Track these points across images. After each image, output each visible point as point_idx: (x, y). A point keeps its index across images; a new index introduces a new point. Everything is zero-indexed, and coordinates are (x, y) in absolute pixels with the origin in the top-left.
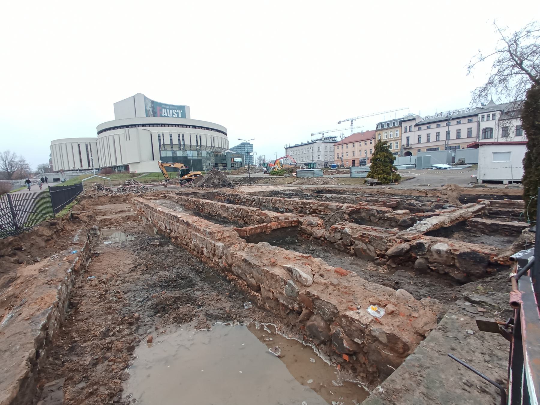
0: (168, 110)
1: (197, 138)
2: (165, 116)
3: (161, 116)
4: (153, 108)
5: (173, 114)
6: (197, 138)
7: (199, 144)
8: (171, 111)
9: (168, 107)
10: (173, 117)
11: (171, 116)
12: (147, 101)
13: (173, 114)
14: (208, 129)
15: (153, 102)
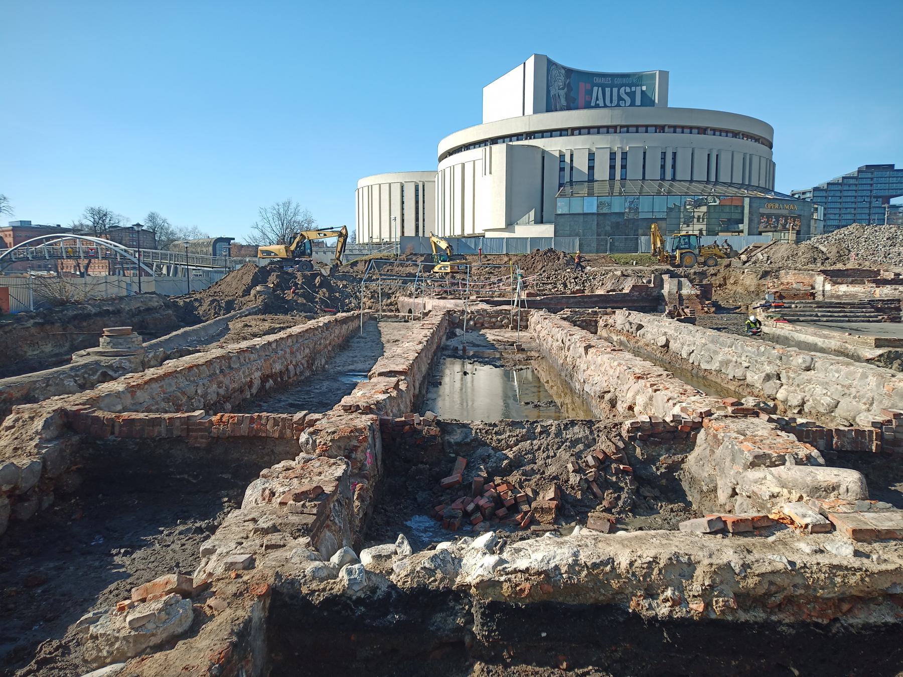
0: (608, 90)
1: (664, 158)
2: (597, 106)
3: (588, 106)
4: (569, 87)
5: (620, 98)
6: (664, 158)
7: (669, 176)
8: (615, 90)
9: (608, 81)
10: (618, 105)
11: (615, 102)
12: (555, 72)
13: (620, 98)
14: (703, 131)
15: (569, 72)
